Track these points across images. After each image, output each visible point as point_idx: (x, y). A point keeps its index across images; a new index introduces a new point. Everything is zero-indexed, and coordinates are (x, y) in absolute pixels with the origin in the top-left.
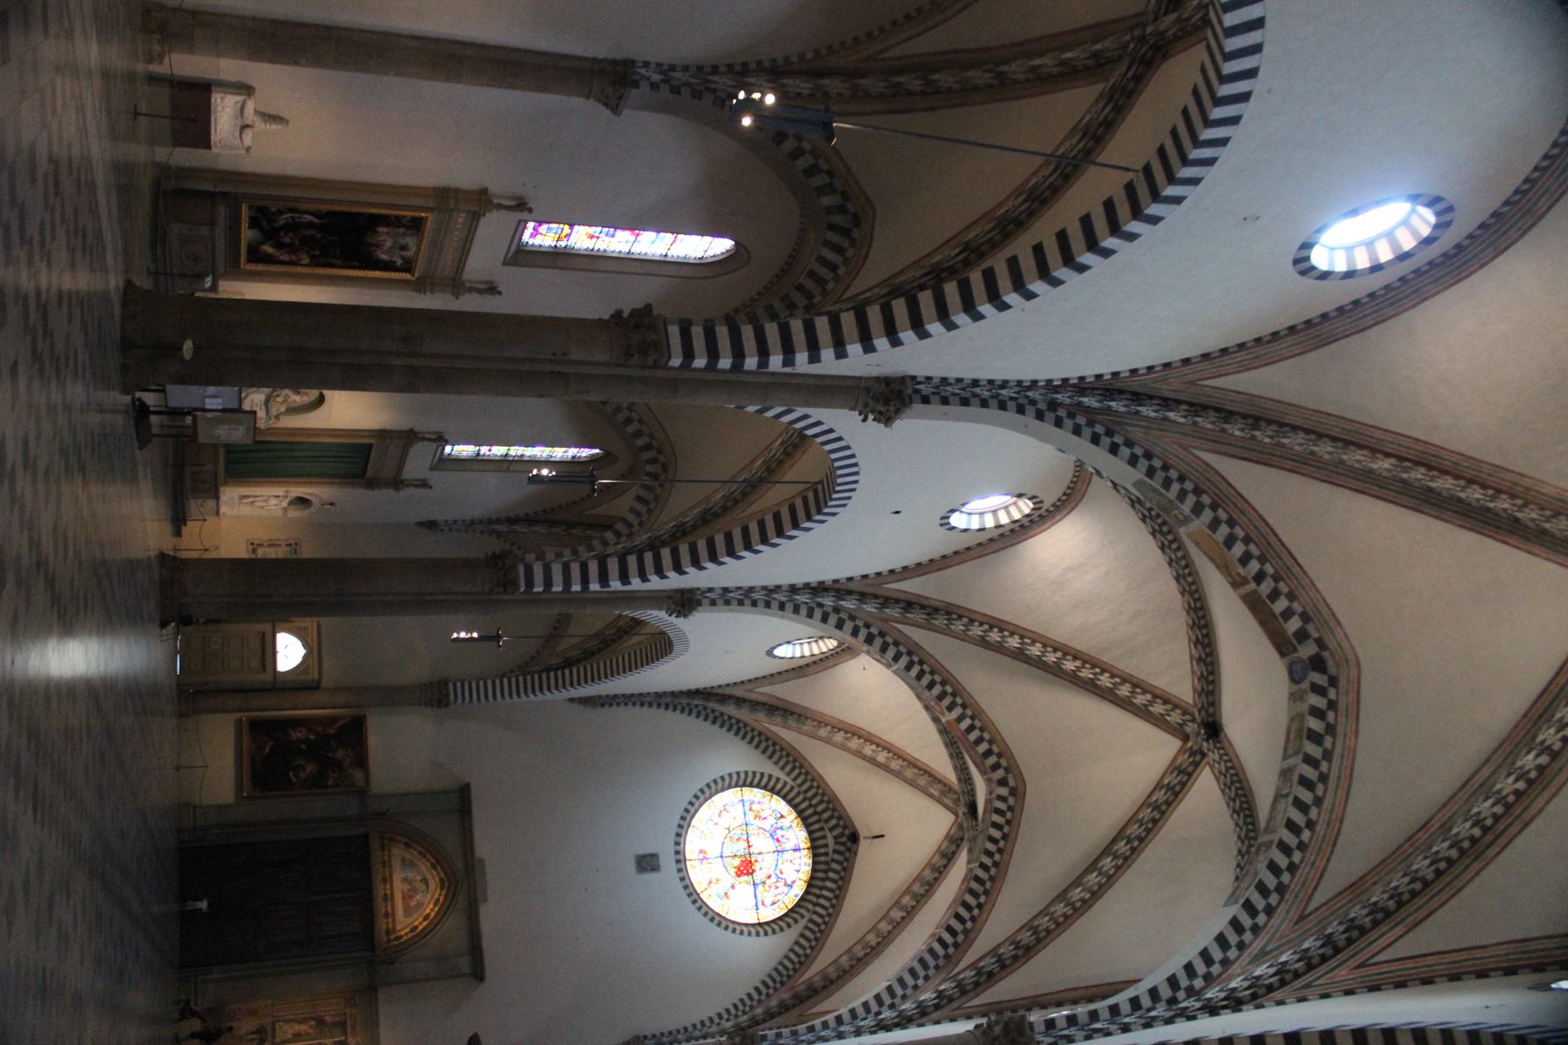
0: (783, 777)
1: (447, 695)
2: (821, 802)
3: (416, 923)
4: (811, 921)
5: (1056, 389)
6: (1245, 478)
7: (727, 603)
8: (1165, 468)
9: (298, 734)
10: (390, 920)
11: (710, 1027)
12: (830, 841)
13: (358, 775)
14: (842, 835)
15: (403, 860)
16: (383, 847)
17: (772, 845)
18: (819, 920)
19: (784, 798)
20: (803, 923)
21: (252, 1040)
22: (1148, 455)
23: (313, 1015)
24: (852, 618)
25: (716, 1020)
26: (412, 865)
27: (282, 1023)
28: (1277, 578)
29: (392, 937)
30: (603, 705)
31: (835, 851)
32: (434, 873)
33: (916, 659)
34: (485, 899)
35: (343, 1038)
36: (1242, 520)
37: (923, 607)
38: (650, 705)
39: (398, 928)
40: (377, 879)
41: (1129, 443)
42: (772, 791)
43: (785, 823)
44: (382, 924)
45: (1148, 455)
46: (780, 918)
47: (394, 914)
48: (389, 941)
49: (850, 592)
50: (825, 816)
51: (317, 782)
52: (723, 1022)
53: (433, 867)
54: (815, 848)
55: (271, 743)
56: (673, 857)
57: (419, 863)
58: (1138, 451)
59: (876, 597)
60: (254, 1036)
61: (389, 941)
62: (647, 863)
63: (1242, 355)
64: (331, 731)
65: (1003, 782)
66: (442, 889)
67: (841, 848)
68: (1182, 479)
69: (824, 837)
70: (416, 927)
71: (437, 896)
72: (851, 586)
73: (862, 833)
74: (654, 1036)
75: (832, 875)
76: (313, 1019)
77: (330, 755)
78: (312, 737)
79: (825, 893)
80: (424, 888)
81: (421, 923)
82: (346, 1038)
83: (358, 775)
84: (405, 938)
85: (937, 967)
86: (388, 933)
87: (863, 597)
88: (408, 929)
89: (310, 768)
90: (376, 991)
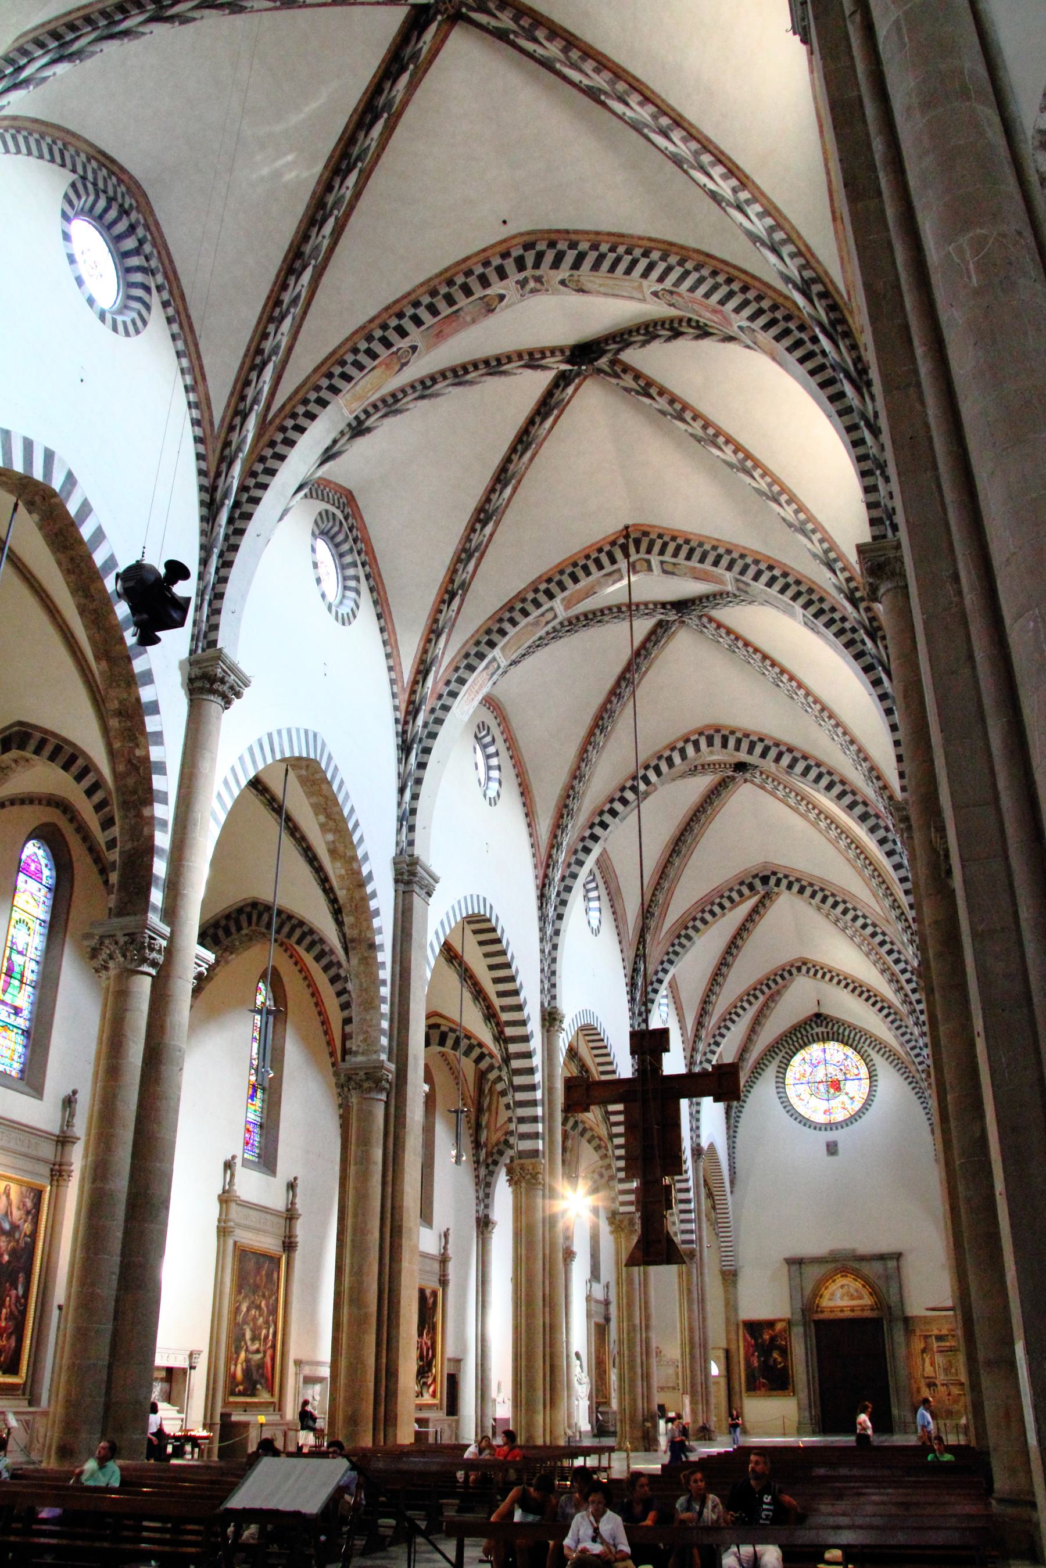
0: (778, 1058)
1: (729, 1271)
2: (795, 1035)
4: (869, 1046)
5: (633, 1014)
6: (673, 915)
7: (698, 1128)
8: (668, 953)
12: (819, 1030)
13: (779, 1326)
14: (816, 1023)
15: (830, 1299)
16: (822, 1312)
17: (821, 1067)
18: (868, 1041)
19: (792, 1057)
20: (870, 1051)
22: (662, 963)
24: (705, 1054)
26: (832, 1294)
28: (722, 897)
31: (826, 1027)
33: (728, 1017)
34: (854, 1250)
36: (694, 914)
37: (701, 1016)
40: (841, 1315)
41: (656, 973)
42: (787, 1065)
43: (807, 1057)
44: (867, 1314)
45: (662, 963)
46: (867, 1065)
49: (692, 1057)
50: (804, 1033)
51: (784, 1351)
53: (834, 1281)
54: (825, 1038)
56: (829, 1133)
58: (660, 968)
59: (695, 1042)
62: (832, 1149)
63: (621, 926)
65: (799, 969)
67: (824, 1023)
68: (673, 945)
69: (817, 1034)
72: (688, 1056)
73: (815, 1010)
75: (841, 1031)
79: (852, 1036)
83: (779, 1326)
85: (901, 1020)
86: (872, 1310)
87: (694, 1049)
89: (775, 1355)
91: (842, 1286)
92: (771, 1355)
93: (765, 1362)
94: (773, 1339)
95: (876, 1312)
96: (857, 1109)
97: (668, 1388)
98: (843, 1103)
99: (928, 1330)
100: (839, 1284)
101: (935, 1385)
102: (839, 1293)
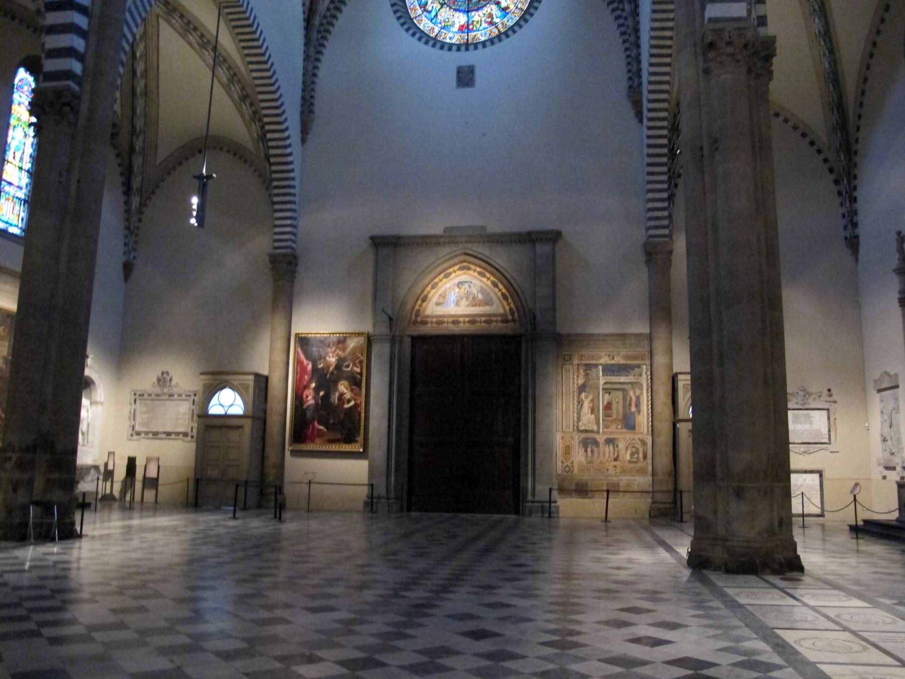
1: (284, 255)
3: (499, 294)
9: (310, 401)
10: (495, 319)
11: (628, 27)
15: (438, 304)
21: (592, 452)
23: (576, 394)
25: (621, 21)
26: (443, 296)
27: (580, 424)
29: (510, 318)
30: (311, 112)
32: (453, 275)
35: (600, 367)
38: (316, 67)
39: (501, 311)
47: (489, 315)
48: (513, 321)
52: (624, 14)
53: (446, 276)
55: (316, 423)
56: (463, 53)
57: (443, 289)
60: (589, 449)
61: (513, 321)
62: (465, 77)
64: (310, 367)
66: (469, 269)
70: (503, 294)
71: (476, 274)
74: (630, 79)
76: (580, 394)
77: (331, 369)
78: (313, 385)
80: (466, 286)
81: (500, 290)
82: (600, 364)
84: (512, 305)
88: (505, 303)
90: (560, 335)
91: (460, 284)
92: (336, 389)
93: (327, 396)
94: (340, 362)
95: (510, 325)
96: (510, 24)
97: (178, 434)
98: (490, 16)
99: (593, 358)
100: (456, 281)
101: (596, 443)
102: (453, 297)
